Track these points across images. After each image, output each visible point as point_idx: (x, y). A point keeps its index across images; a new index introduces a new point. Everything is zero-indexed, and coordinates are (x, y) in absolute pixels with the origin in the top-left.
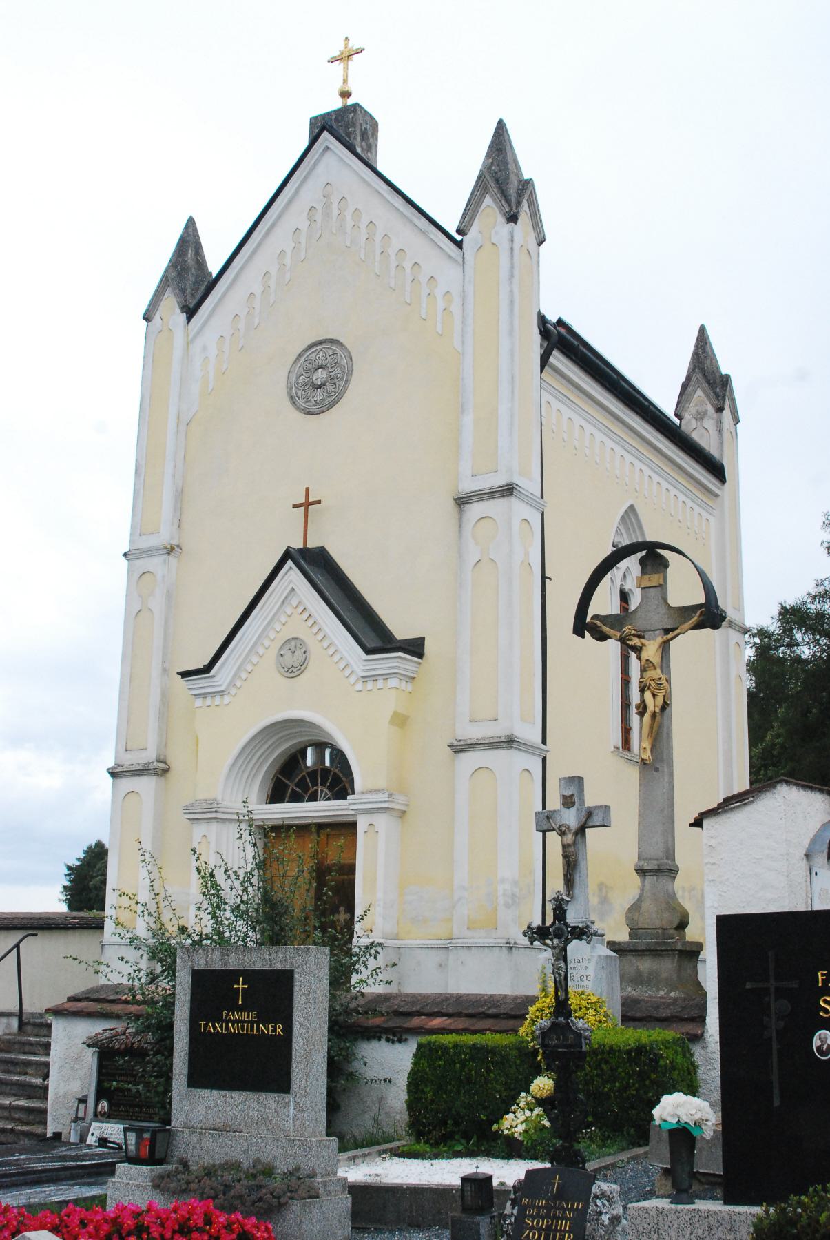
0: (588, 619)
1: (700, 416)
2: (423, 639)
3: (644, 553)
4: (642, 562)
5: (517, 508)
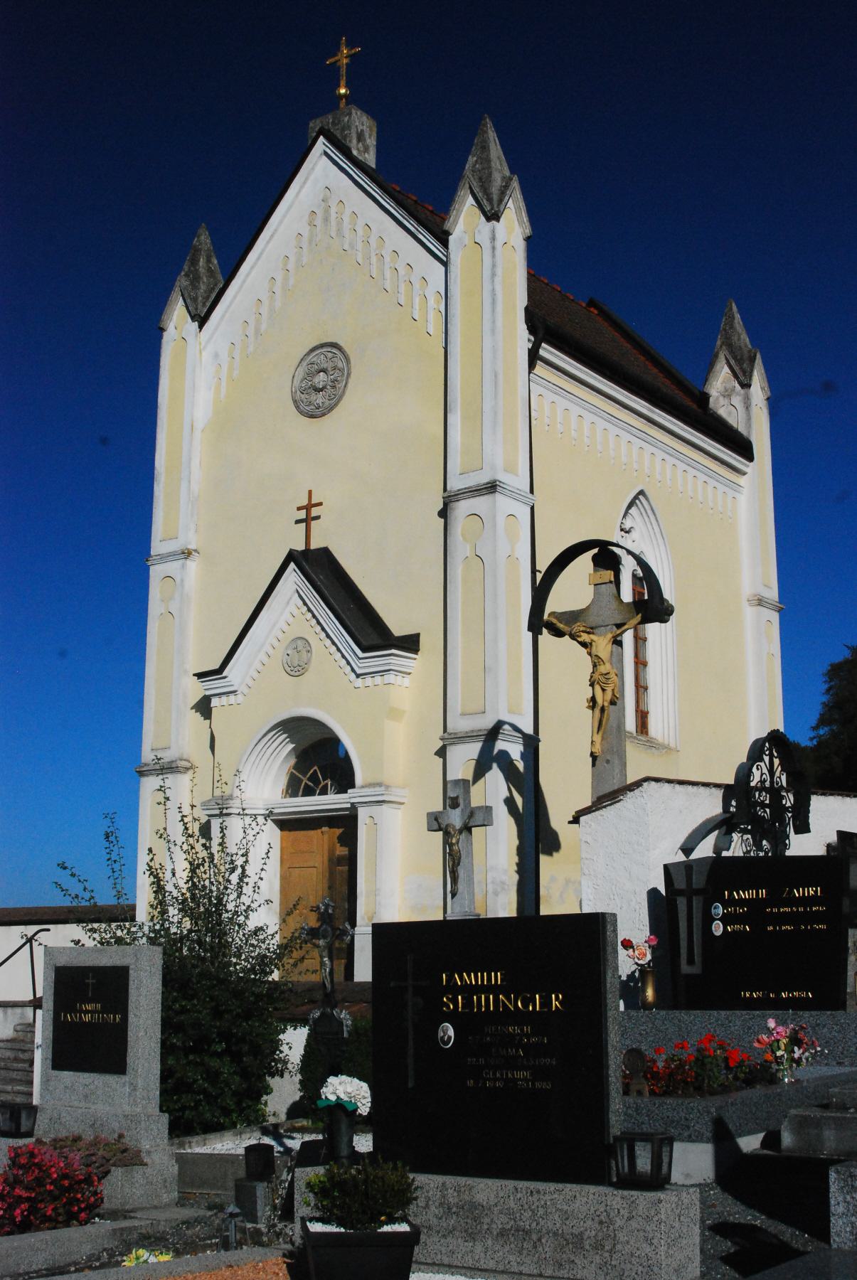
0: (546, 617)
1: (727, 394)
2: (418, 635)
3: (596, 551)
4: (595, 558)
5: (501, 501)
